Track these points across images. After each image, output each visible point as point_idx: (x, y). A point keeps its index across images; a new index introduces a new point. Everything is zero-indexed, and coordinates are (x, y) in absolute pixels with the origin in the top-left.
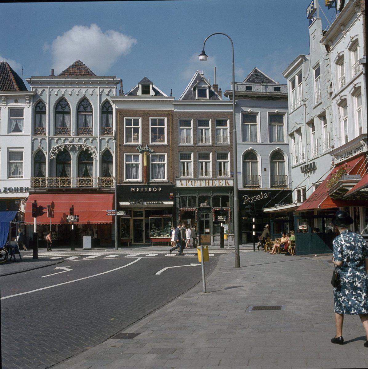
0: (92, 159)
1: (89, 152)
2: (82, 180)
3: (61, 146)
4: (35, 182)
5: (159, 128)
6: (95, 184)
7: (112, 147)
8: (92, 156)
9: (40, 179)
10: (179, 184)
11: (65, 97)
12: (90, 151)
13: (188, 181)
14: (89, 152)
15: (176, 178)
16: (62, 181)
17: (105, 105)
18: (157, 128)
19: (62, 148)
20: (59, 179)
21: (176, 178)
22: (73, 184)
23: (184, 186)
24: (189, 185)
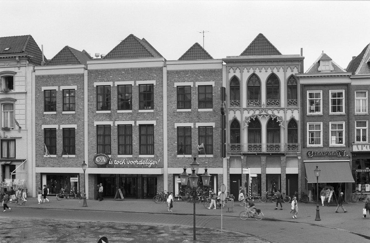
0: (279, 127)
1: (277, 121)
2: (272, 145)
3: (253, 116)
4: (231, 147)
5: (337, 99)
6: (283, 149)
7: (297, 115)
8: (279, 125)
9: (236, 144)
10: (355, 149)
11: (256, 73)
12: (278, 120)
13: (363, 146)
14: (277, 121)
15: (353, 144)
16: (255, 147)
17: (290, 80)
18: (336, 99)
19: (274, 118)
20: (253, 144)
21: (353, 144)
22: (264, 149)
23: (360, 150)
24: (365, 149)
